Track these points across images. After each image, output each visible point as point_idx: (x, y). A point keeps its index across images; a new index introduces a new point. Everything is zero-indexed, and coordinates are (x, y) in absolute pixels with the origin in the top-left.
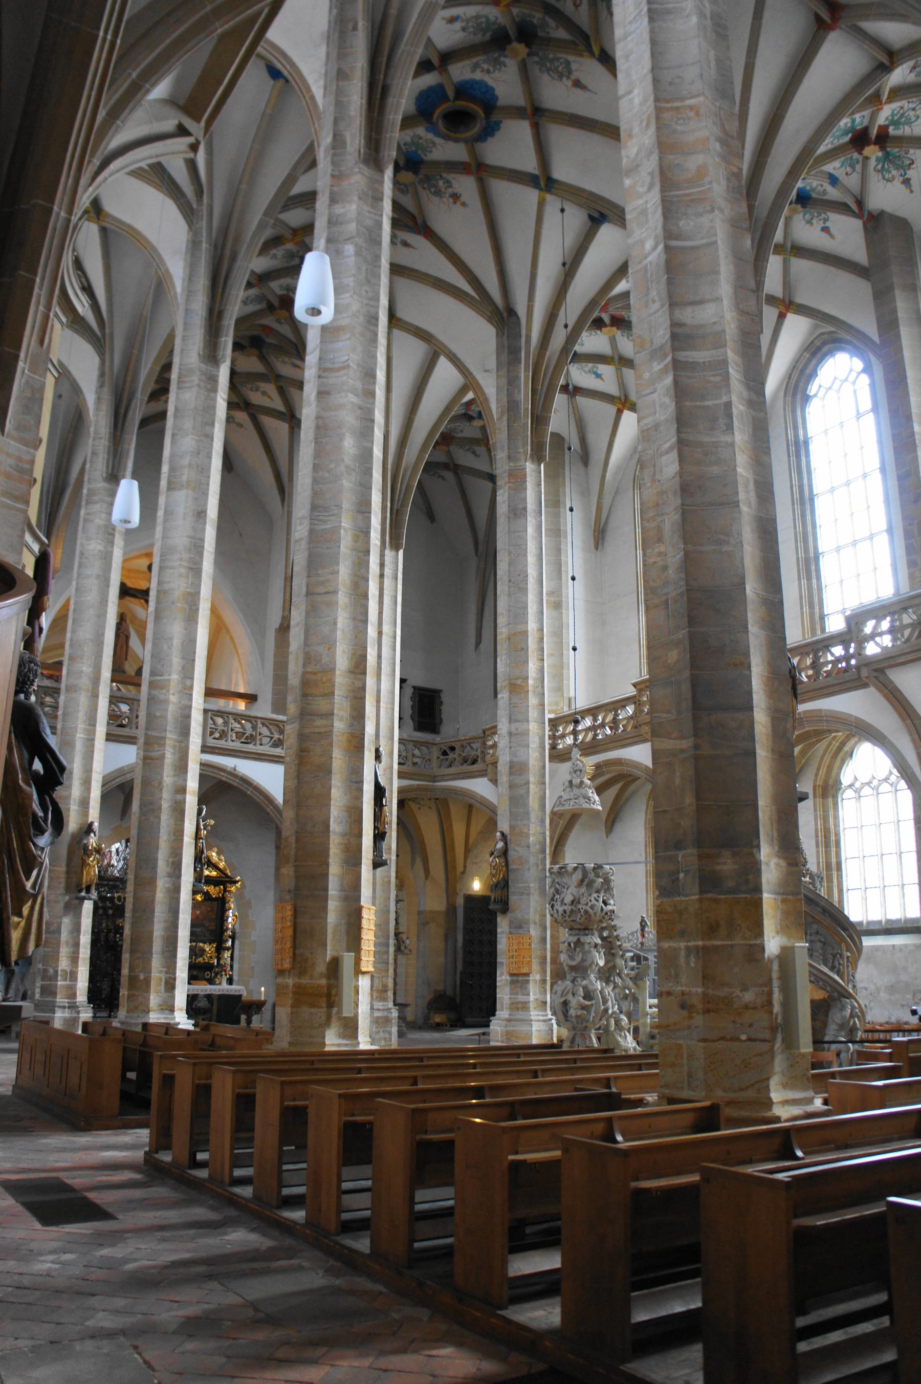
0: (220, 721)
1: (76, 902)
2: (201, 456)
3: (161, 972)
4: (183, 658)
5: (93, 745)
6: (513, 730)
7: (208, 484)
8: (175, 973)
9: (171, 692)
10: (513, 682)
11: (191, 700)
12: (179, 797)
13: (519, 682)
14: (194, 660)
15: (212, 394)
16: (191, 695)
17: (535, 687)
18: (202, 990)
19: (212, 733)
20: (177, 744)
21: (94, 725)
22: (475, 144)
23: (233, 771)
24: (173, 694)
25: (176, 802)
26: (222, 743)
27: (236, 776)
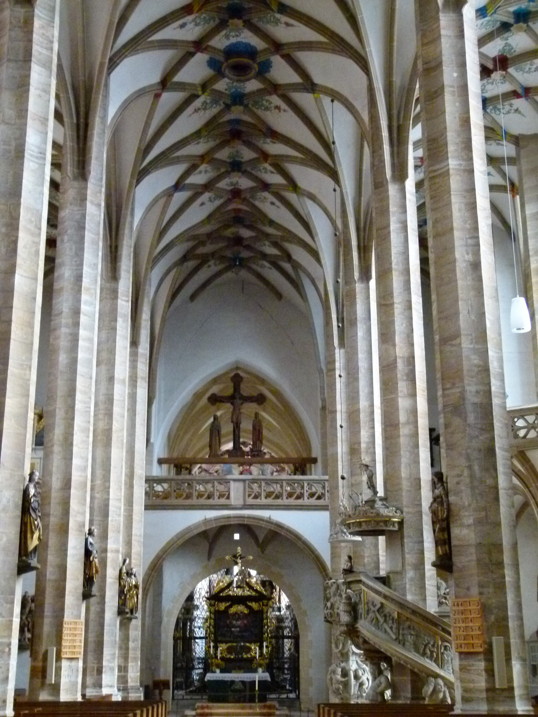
0: (255, 486)
1: (126, 621)
2: (110, 343)
3: (94, 663)
4: (103, 470)
5: (132, 519)
6: (353, 482)
7: (115, 359)
8: (102, 664)
9: (96, 492)
10: (352, 447)
11: (109, 494)
12: (103, 555)
13: (356, 446)
14: (110, 470)
15: (115, 301)
16: (109, 492)
17: (368, 448)
18: (238, 678)
19: (249, 495)
20: (101, 523)
21: (132, 506)
22: (267, 75)
23: (269, 520)
24: (98, 493)
25: (102, 558)
26: (258, 501)
27: (271, 523)
